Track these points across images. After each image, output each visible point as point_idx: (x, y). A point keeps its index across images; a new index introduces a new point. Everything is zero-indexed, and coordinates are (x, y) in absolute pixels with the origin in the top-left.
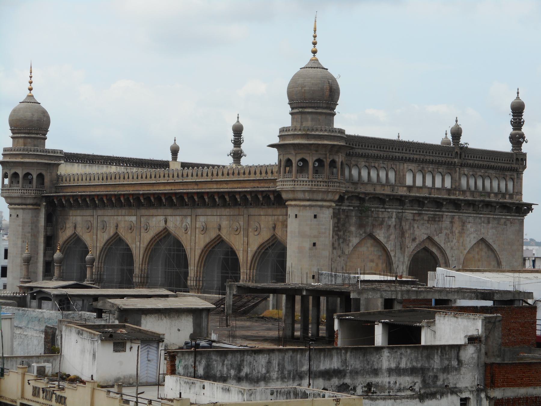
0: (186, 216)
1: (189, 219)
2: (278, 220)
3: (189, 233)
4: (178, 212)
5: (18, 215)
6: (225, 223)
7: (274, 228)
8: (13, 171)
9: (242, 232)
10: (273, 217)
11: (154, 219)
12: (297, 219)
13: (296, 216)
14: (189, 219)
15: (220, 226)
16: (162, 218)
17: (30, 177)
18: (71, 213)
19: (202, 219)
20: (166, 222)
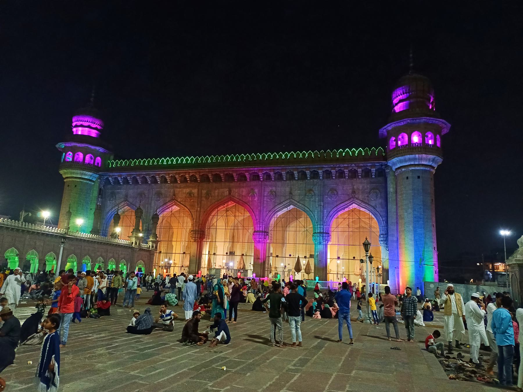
3: (256, 199)
5: (76, 186)
12: (421, 180)
13: (419, 177)
16: (227, 189)
20: (230, 193)
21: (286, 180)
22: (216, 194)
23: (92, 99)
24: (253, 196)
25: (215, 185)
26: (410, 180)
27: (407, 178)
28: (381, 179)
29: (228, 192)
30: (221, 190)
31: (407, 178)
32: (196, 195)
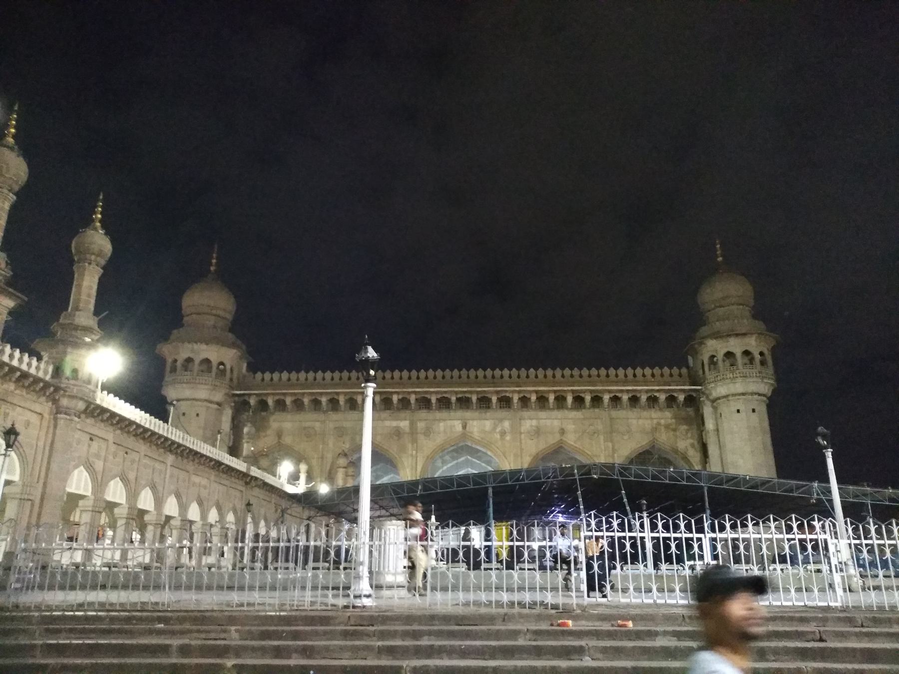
0: (501, 420)
1: (507, 424)
2: (659, 424)
3: (508, 438)
4: (489, 414)
5: (198, 415)
6: (570, 427)
7: (655, 429)
8: (204, 355)
9: (602, 437)
10: (649, 421)
11: (442, 424)
13: (754, 411)
14: (507, 424)
15: (563, 429)
16: (459, 422)
17: (221, 367)
18: (272, 418)
19: (534, 422)
20: (464, 427)
21: (553, 409)
22: (442, 429)
23: (212, 268)
24: (503, 434)
25: (438, 415)
26: (743, 414)
27: (738, 411)
28: (690, 411)
29: (460, 426)
30: (449, 423)
31: (738, 411)
32: (407, 430)
